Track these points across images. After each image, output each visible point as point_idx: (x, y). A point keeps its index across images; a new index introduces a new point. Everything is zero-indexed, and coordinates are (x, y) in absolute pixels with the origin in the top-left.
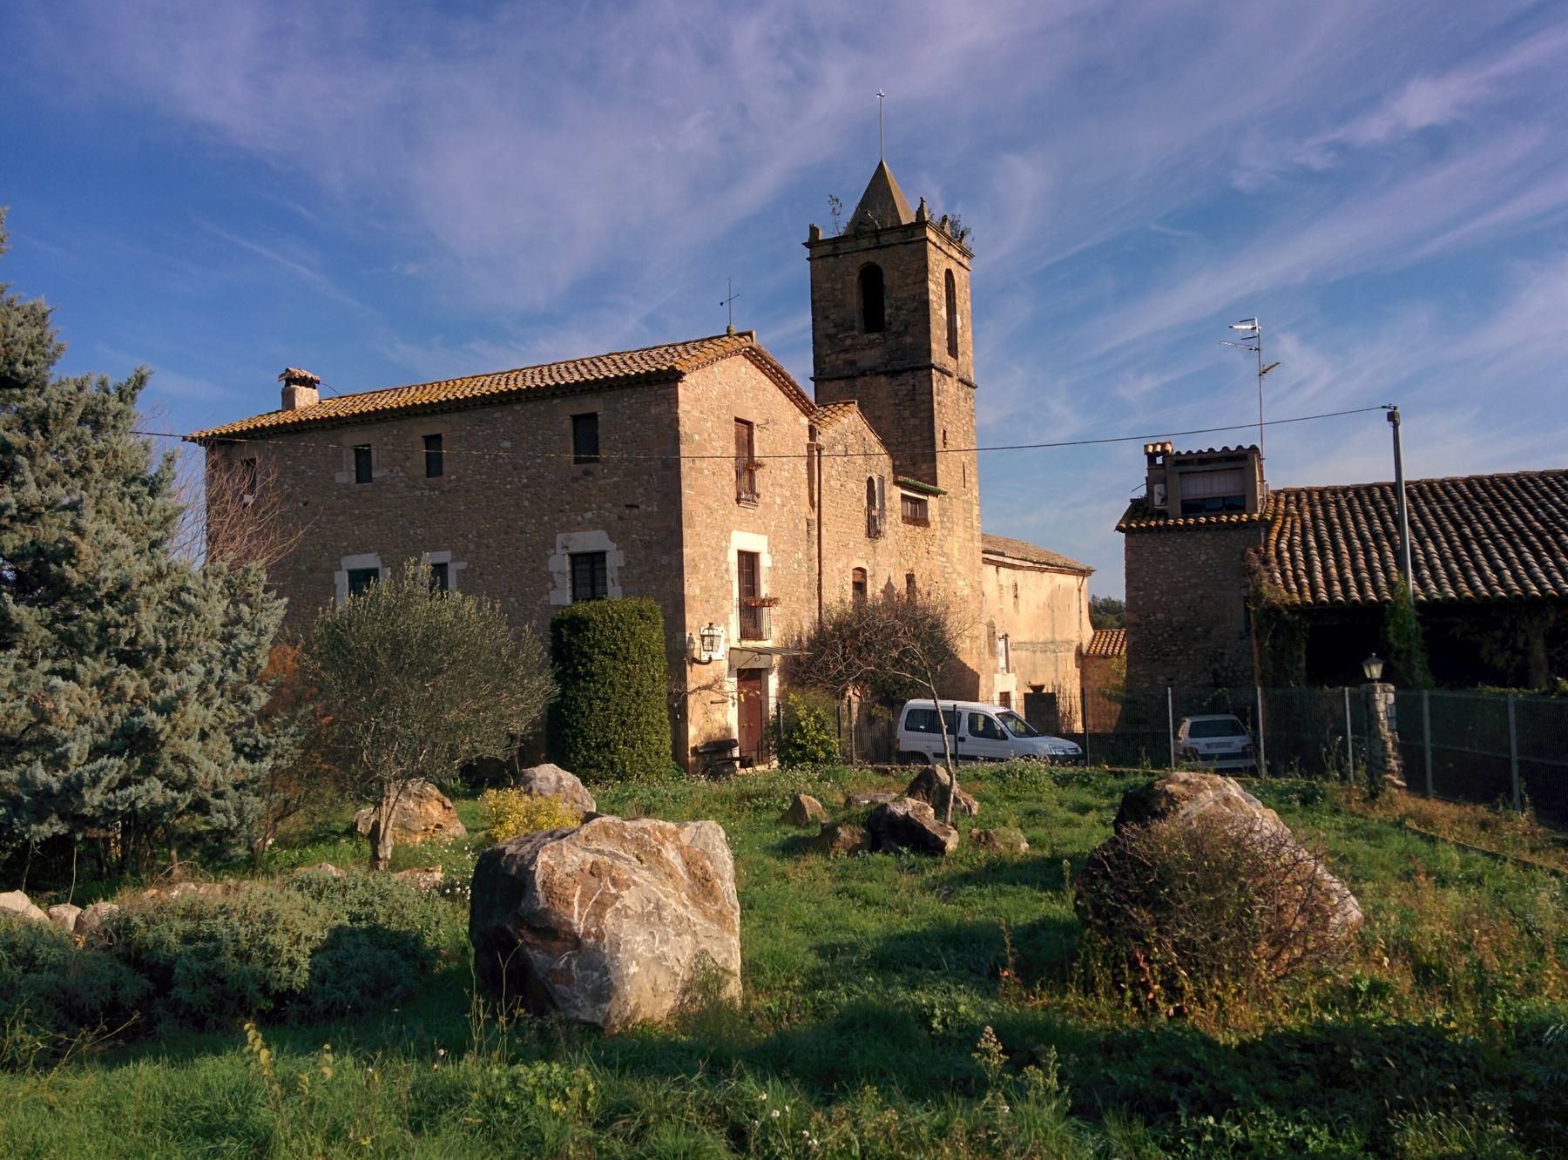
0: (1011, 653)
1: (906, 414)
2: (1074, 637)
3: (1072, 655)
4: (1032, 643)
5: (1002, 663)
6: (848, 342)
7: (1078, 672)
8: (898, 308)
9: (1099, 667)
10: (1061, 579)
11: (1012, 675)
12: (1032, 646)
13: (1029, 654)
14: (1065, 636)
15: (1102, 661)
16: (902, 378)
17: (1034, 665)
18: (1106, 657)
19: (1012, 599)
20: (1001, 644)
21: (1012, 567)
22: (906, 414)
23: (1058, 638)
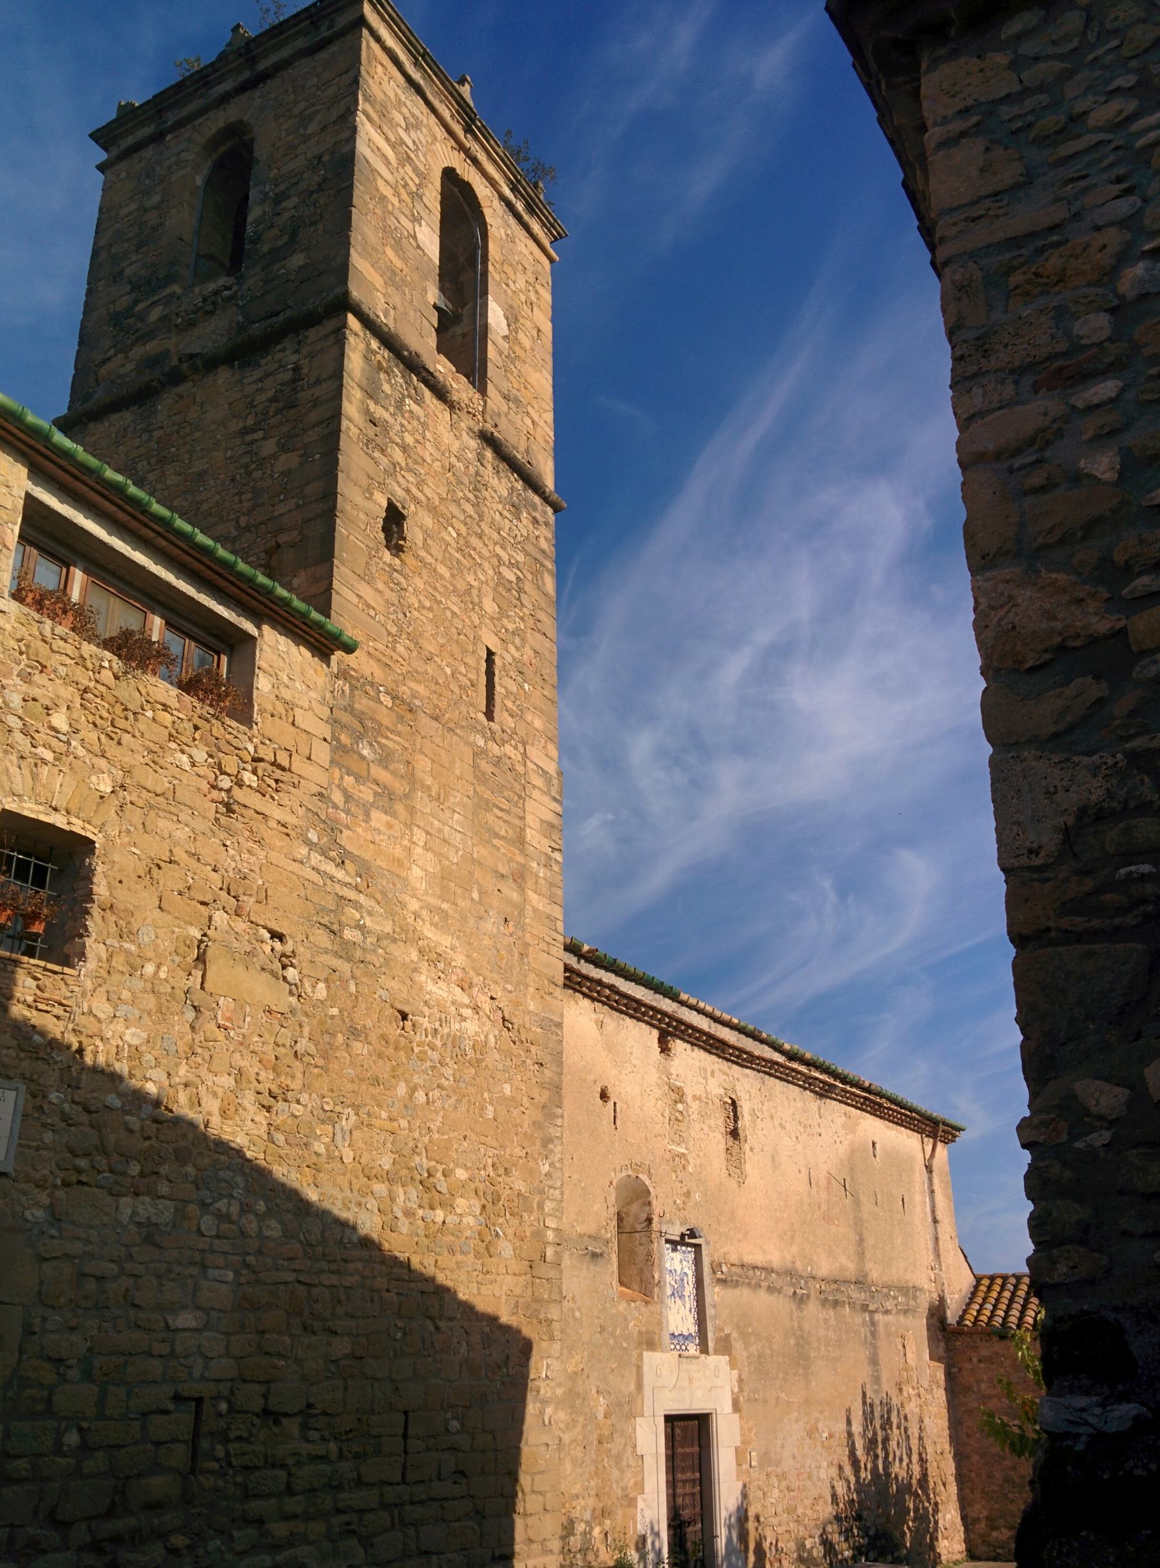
0: (713, 1293)
1: (269, 447)
2: (922, 1278)
3: (917, 1328)
4: (790, 1273)
5: (679, 1317)
6: (155, 314)
7: (939, 1372)
8: (279, 199)
9: (989, 1360)
10: (873, 1127)
11: (717, 1361)
12: (793, 1283)
13: (781, 1304)
14: (897, 1273)
15: (997, 1346)
16: (268, 362)
17: (802, 1339)
18: (1003, 1334)
19: (718, 1140)
20: (676, 1264)
21: (715, 1046)
22: (269, 447)
23: (875, 1274)
